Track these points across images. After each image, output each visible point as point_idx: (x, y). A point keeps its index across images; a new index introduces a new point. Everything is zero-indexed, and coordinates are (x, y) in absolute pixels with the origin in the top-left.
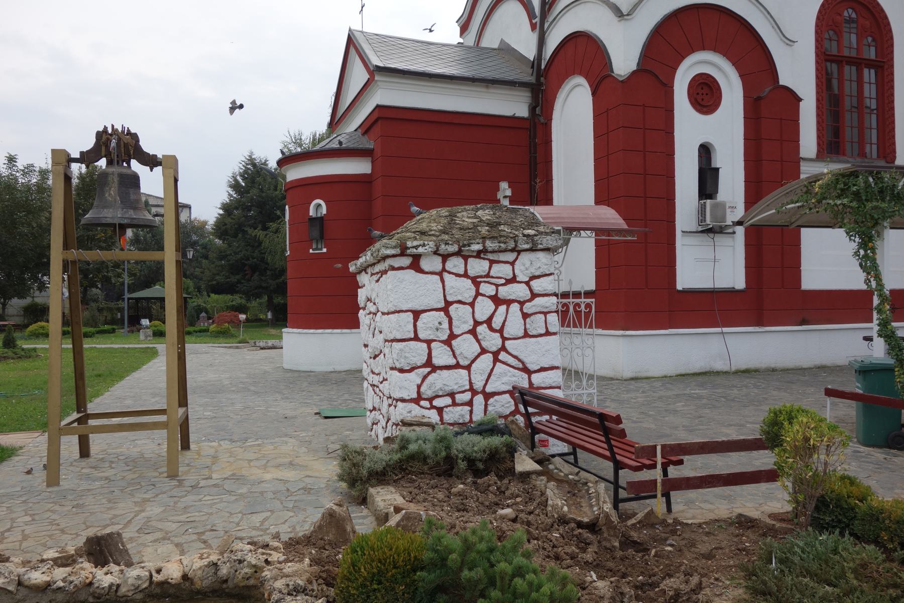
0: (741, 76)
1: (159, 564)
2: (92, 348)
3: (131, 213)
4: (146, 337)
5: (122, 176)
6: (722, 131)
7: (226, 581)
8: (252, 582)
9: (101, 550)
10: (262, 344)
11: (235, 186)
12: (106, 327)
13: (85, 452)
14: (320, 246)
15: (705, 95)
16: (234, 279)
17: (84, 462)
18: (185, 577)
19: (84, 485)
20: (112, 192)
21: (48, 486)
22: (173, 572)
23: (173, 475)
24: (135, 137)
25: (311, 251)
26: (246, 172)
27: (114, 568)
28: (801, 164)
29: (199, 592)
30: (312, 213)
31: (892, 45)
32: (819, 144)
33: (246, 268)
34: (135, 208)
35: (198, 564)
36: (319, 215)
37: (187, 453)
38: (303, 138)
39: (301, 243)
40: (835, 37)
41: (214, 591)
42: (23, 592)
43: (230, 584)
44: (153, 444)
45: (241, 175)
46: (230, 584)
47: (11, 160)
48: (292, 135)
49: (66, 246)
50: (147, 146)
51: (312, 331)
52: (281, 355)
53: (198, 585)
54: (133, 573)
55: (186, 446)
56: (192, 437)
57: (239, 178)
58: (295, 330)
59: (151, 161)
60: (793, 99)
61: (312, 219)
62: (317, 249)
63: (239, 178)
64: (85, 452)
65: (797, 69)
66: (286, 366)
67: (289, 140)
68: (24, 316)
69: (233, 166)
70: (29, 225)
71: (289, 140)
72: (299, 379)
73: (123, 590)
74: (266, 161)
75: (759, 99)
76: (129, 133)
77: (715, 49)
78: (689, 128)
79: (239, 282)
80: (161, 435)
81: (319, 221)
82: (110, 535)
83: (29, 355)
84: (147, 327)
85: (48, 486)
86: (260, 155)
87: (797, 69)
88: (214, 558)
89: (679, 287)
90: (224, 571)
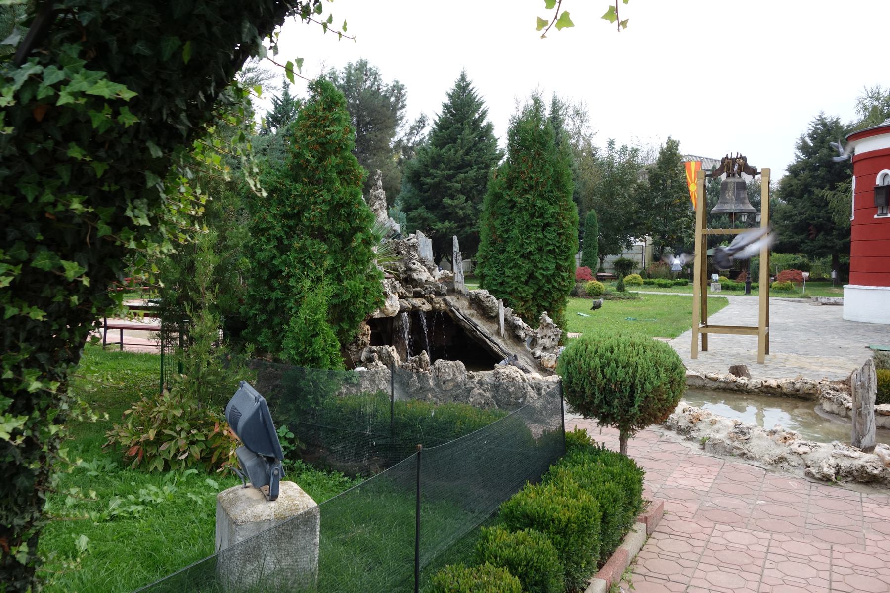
1: (765, 379)
2: (676, 296)
3: (741, 206)
4: (716, 289)
5: (738, 183)
7: (798, 391)
8: (812, 392)
9: (737, 370)
10: (824, 300)
11: (804, 148)
12: (681, 280)
13: (704, 349)
14: (885, 212)
16: (797, 239)
17: (705, 353)
18: (778, 386)
19: (711, 361)
20: (730, 195)
21: (692, 358)
22: (773, 383)
23: (761, 362)
24: (744, 159)
25: (876, 216)
26: (815, 132)
27: (746, 378)
29: (785, 394)
30: (878, 182)
33: (811, 228)
34: (743, 203)
35: (784, 382)
36: (886, 184)
37: (767, 356)
38: (881, 91)
39: (865, 209)
41: (792, 395)
42: (707, 381)
43: (801, 392)
44: (749, 344)
45: (811, 137)
46: (801, 392)
47: (611, 143)
48: (869, 89)
49: (703, 227)
50: (750, 163)
51: (872, 287)
52: (842, 310)
53: (785, 390)
54: (753, 381)
55: (767, 352)
56: (770, 350)
57: (808, 140)
58: (856, 286)
59: (753, 172)
61: (878, 189)
62: (882, 214)
63: (808, 140)
64: (704, 349)
66: (845, 317)
67: (865, 96)
68: (615, 269)
69: (802, 127)
70: (623, 195)
71: (865, 96)
72: (855, 327)
73: (749, 387)
74: (838, 119)
76: (741, 157)
79: (802, 241)
80: (756, 338)
82: (742, 366)
83: (633, 297)
84: (717, 281)
85: (692, 358)
86: (830, 115)
88: (793, 381)
90: (798, 386)
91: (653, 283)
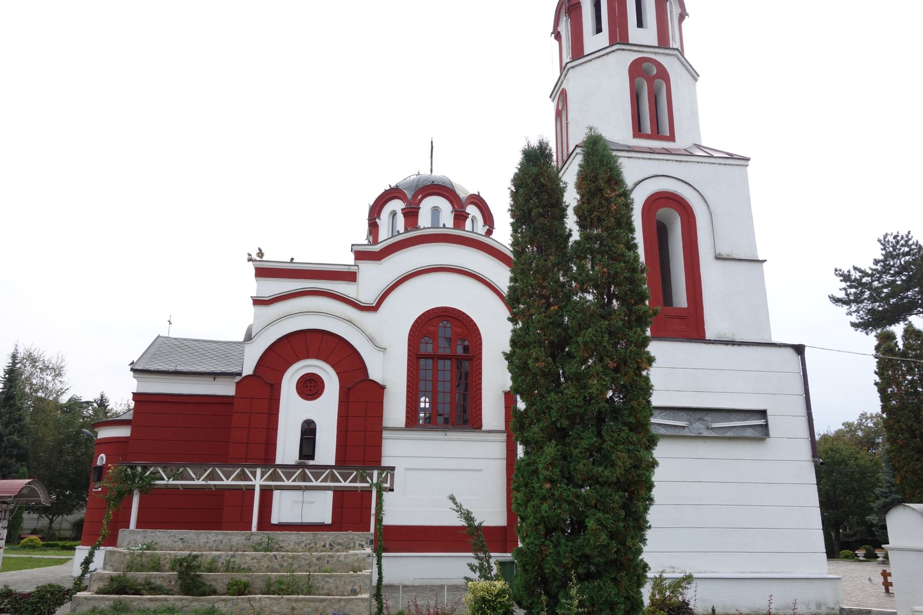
0: (338, 374)
6: (325, 411)
15: (310, 387)
28: (384, 432)
31: (481, 344)
32: (407, 417)
40: (431, 341)
60: (378, 390)
65: (389, 368)
70: (74, 453)
75: (349, 389)
77: (317, 357)
78: (292, 410)
81: (101, 467)
87: (389, 368)
89: (274, 521)
91: (57, 545)
